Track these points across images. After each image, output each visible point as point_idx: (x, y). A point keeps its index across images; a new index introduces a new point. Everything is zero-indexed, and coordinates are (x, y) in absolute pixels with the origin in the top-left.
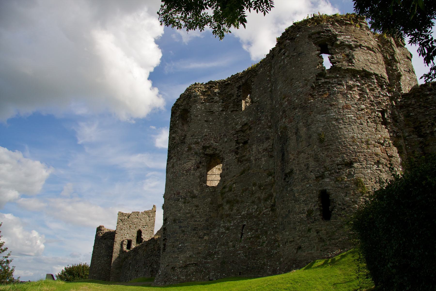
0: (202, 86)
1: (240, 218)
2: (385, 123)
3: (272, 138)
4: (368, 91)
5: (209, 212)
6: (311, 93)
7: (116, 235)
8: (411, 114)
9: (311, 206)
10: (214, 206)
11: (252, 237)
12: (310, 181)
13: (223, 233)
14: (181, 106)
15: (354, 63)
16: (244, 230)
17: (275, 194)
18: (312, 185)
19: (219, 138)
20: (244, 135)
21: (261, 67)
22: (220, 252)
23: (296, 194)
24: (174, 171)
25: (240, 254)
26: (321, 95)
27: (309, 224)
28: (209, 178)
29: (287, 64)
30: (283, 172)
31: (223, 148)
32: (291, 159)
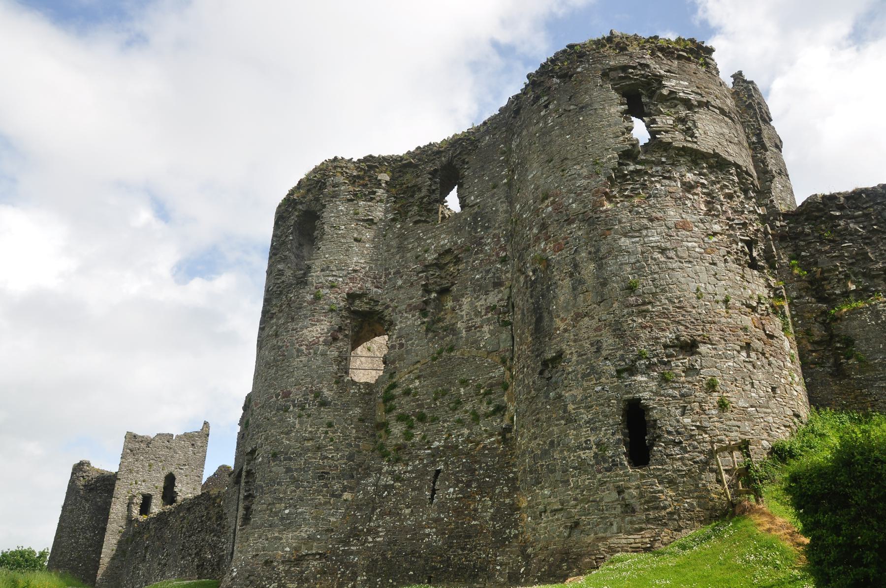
0: (349, 164)
1: (428, 454)
2: (753, 265)
3: (507, 284)
4: (722, 197)
5: (356, 438)
6: (607, 190)
7: (117, 482)
8: (803, 254)
9: (605, 434)
10: (367, 427)
11: (457, 499)
12: (603, 380)
13: (386, 487)
14: (301, 203)
15: (696, 137)
16: (438, 483)
17: (511, 407)
18: (607, 388)
19: (383, 279)
20: (443, 275)
21: (487, 132)
22: (380, 529)
23: (571, 407)
24: (280, 344)
25: (429, 535)
26: (627, 196)
27: (600, 472)
28: (355, 363)
29: (553, 127)
30: (537, 356)
31: (392, 300)
32: (558, 329)
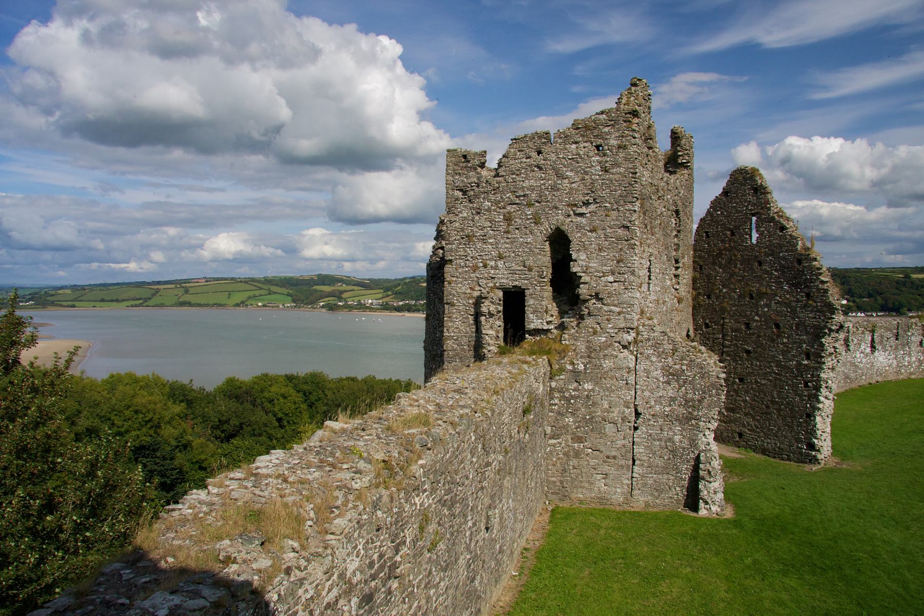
7: (448, 268)
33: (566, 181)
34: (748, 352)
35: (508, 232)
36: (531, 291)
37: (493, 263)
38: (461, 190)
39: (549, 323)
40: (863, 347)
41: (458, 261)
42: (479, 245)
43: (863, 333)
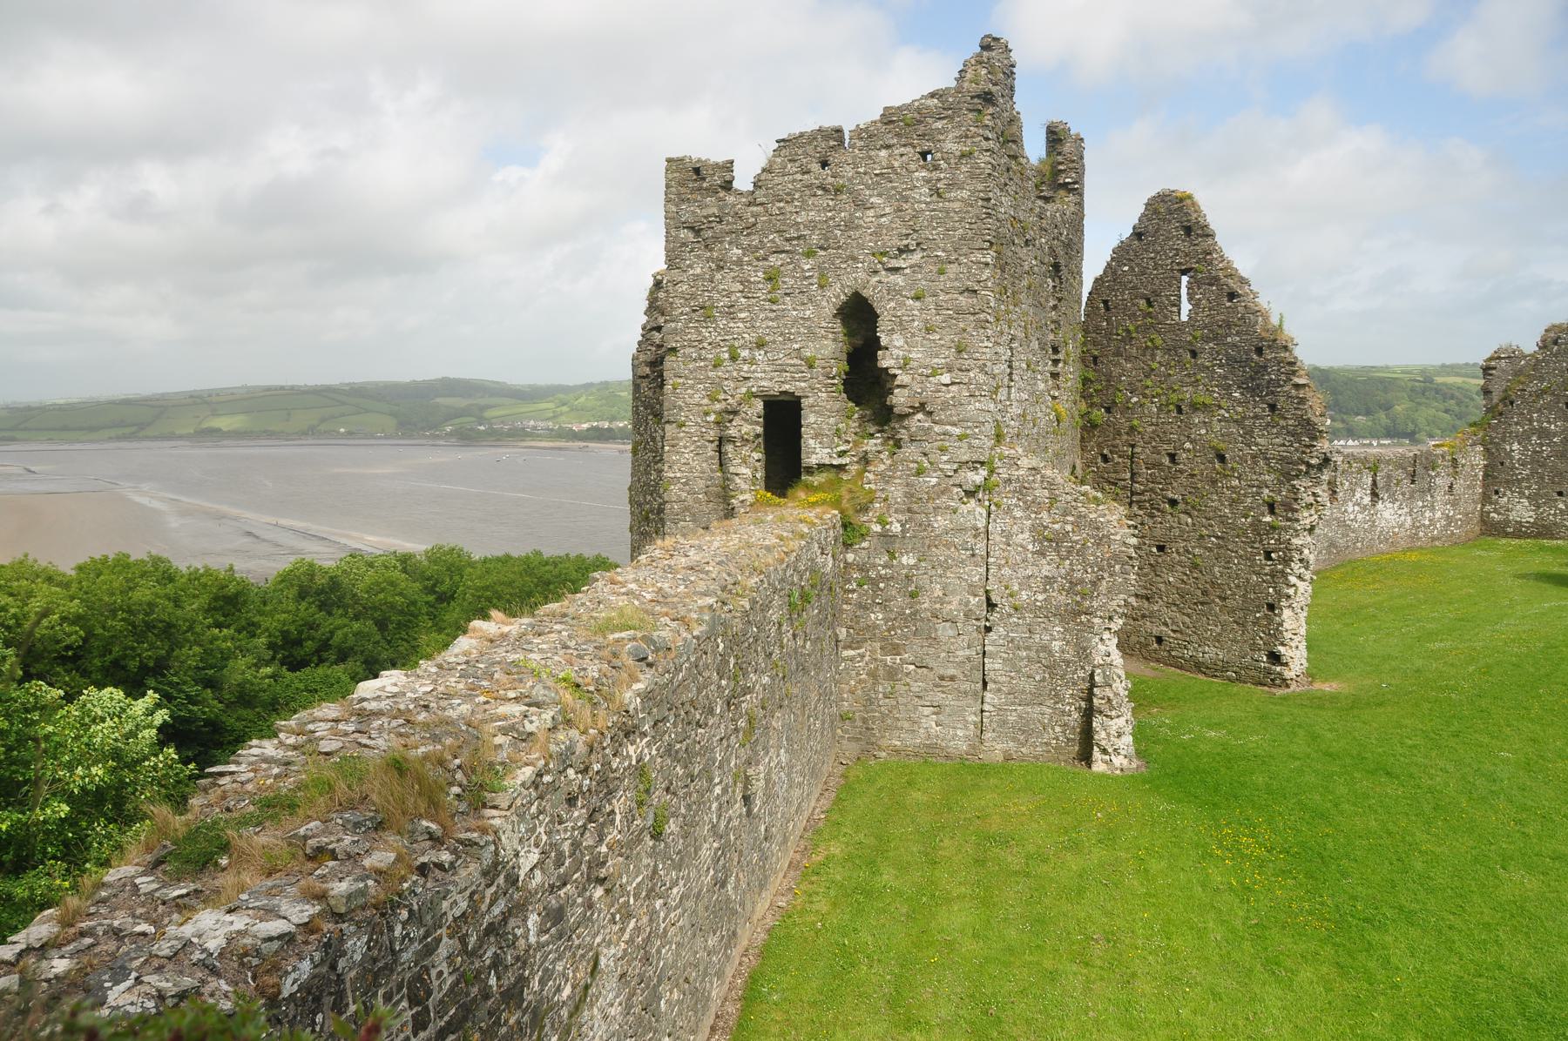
7: (669, 362)
33: (871, 213)
34: (1173, 503)
35: (773, 302)
36: (811, 400)
37: (745, 353)
38: (692, 228)
39: (842, 454)
40: (1358, 495)
41: (688, 350)
42: (722, 323)
43: (1359, 472)
